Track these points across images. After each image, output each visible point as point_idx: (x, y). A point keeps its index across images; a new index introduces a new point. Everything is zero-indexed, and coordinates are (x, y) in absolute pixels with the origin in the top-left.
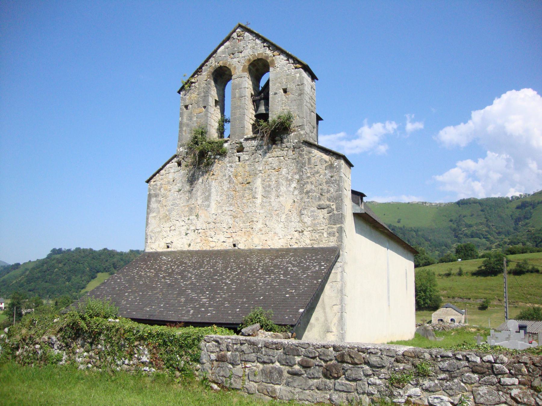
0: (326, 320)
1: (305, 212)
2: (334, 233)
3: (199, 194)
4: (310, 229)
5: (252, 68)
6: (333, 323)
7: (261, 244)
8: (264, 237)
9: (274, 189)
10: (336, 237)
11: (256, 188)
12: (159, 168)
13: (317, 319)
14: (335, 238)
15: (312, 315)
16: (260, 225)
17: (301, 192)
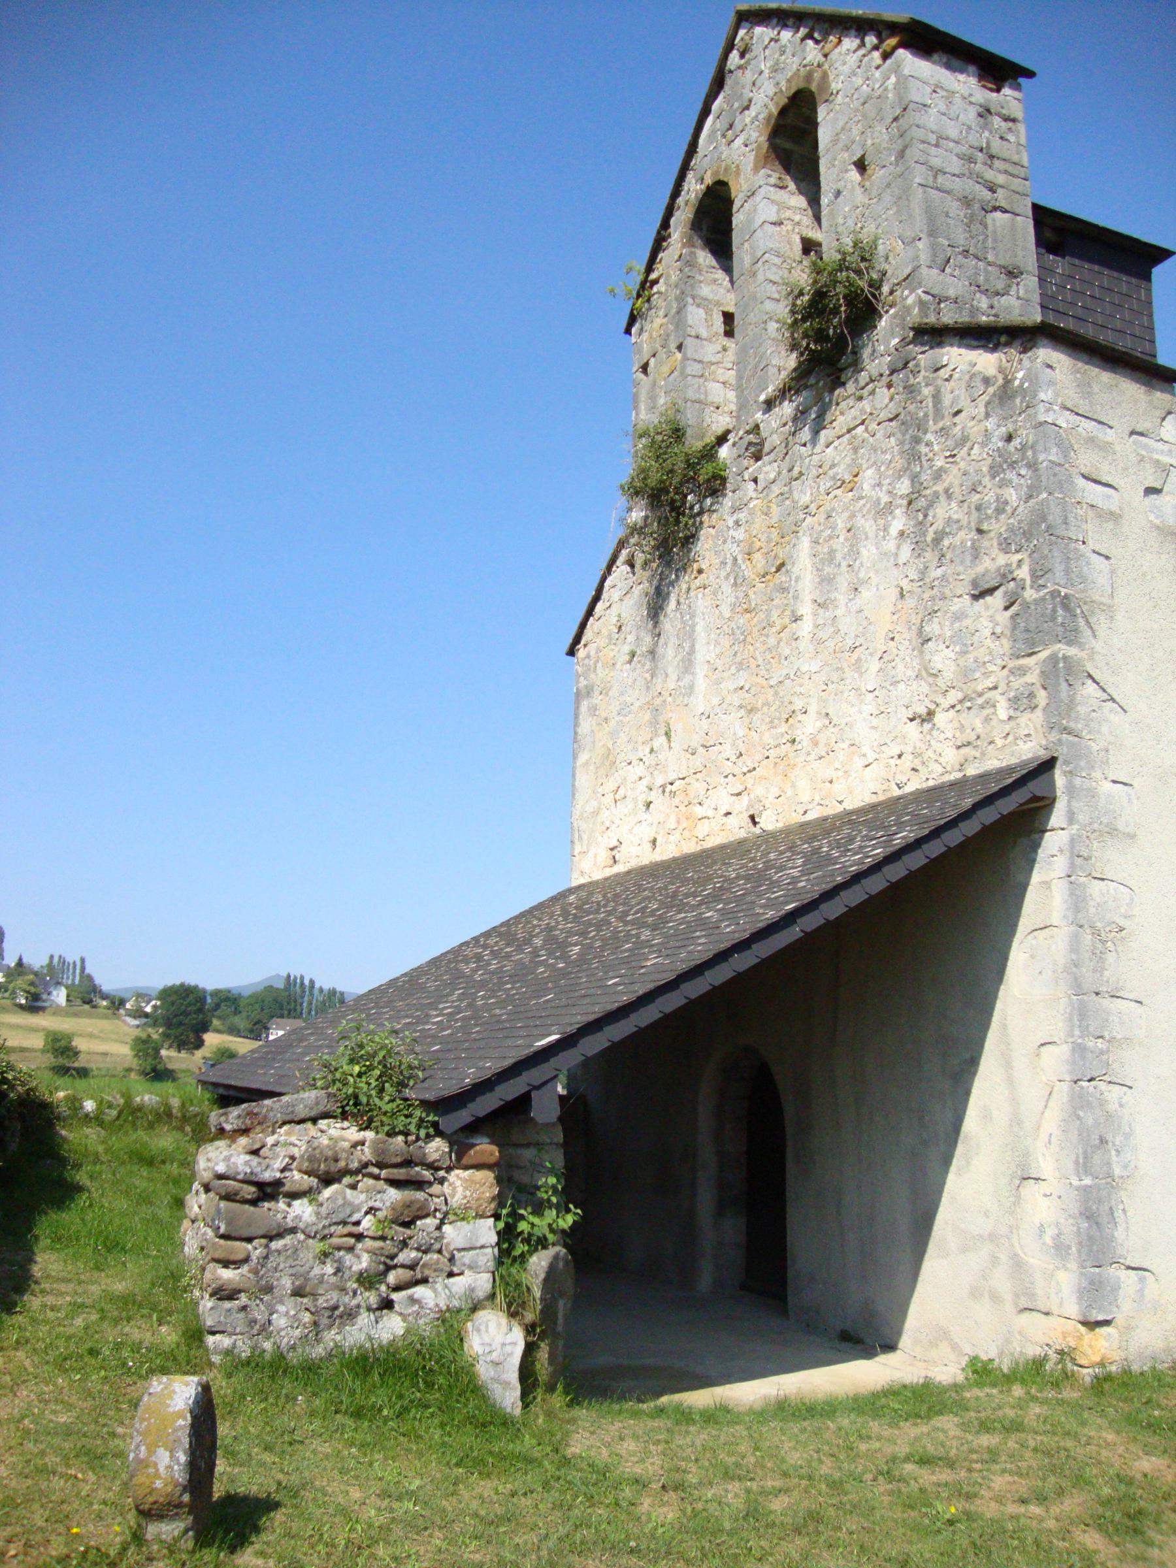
0: (1016, 1120)
1: (932, 628)
2: (1031, 695)
3: (670, 652)
4: (954, 696)
5: (789, 145)
6: (1043, 1137)
7: (817, 799)
8: (824, 770)
9: (844, 564)
10: (1039, 712)
11: (798, 579)
12: (589, 599)
13: (986, 1116)
14: (1038, 716)
15: (968, 1093)
16: (809, 726)
17: (919, 547)
